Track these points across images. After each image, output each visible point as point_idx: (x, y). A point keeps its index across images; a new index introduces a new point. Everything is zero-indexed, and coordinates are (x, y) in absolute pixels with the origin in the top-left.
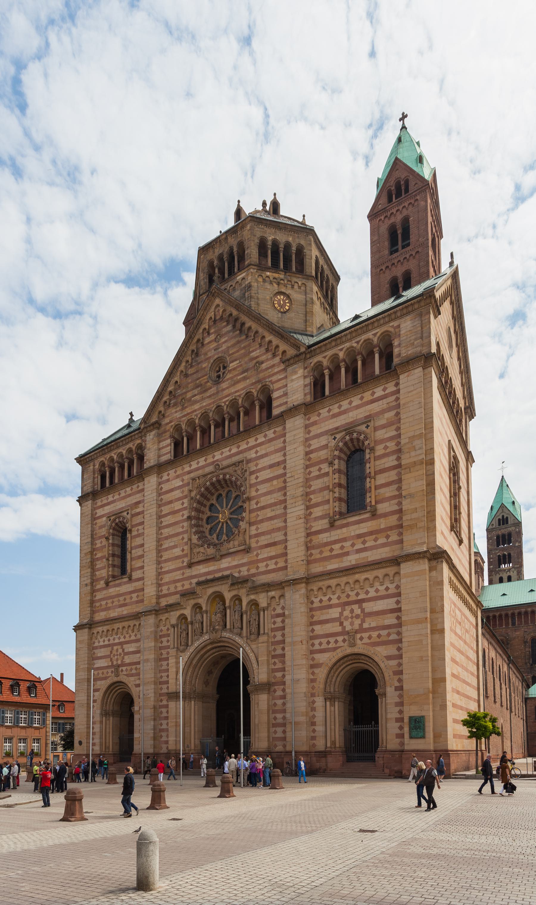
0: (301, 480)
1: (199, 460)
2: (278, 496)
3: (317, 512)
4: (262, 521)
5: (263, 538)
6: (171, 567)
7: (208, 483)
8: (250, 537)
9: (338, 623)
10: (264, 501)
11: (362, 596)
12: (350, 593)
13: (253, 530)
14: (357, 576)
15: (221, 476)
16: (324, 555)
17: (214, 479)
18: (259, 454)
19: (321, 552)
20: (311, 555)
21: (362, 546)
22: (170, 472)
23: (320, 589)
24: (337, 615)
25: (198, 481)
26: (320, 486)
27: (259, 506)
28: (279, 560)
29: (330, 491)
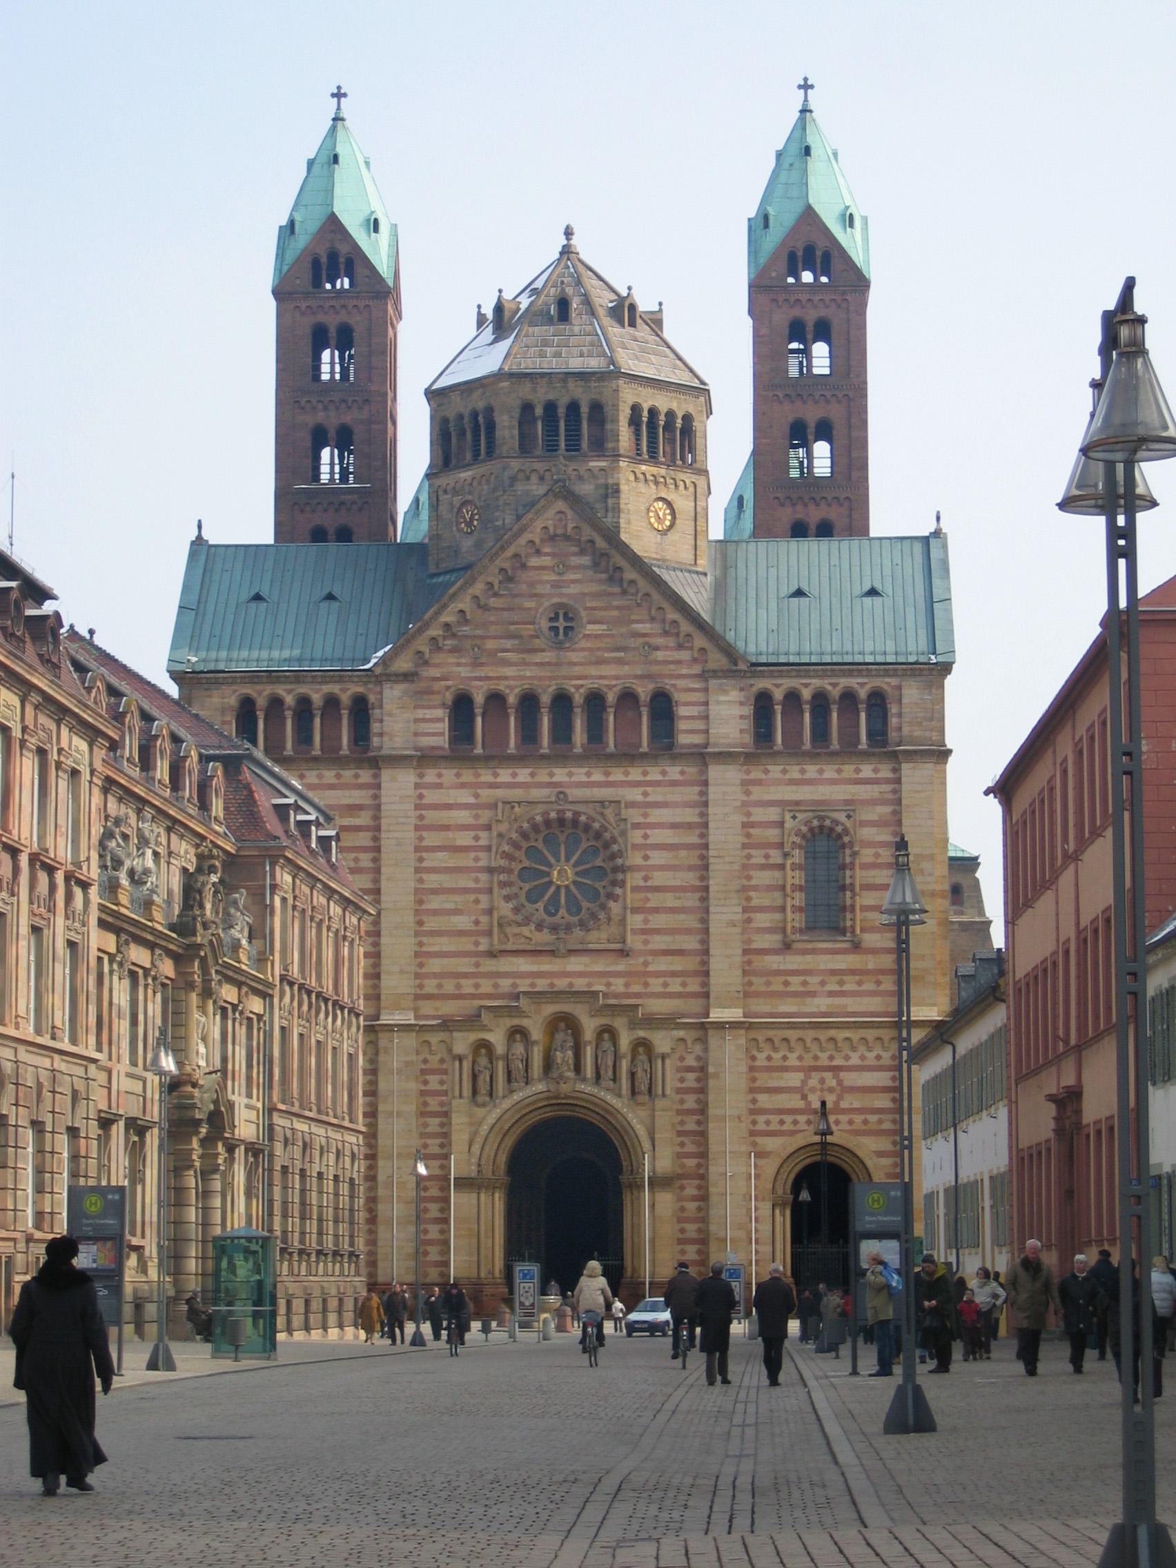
0: (736, 867)
1: (518, 771)
2: (691, 878)
3: (762, 920)
4: (656, 910)
5: (657, 938)
6: (452, 948)
7: (539, 818)
8: (634, 931)
9: (798, 1096)
10: (659, 879)
11: (838, 1062)
12: (819, 1054)
13: (635, 921)
14: (832, 1033)
15: (569, 815)
16: (774, 988)
17: (553, 815)
18: (649, 799)
19: (768, 983)
20: (750, 984)
21: (837, 988)
22: (444, 771)
23: (770, 1040)
24: (798, 1084)
25: (517, 809)
26: (767, 882)
27: (649, 884)
28: (688, 980)
29: (785, 895)
